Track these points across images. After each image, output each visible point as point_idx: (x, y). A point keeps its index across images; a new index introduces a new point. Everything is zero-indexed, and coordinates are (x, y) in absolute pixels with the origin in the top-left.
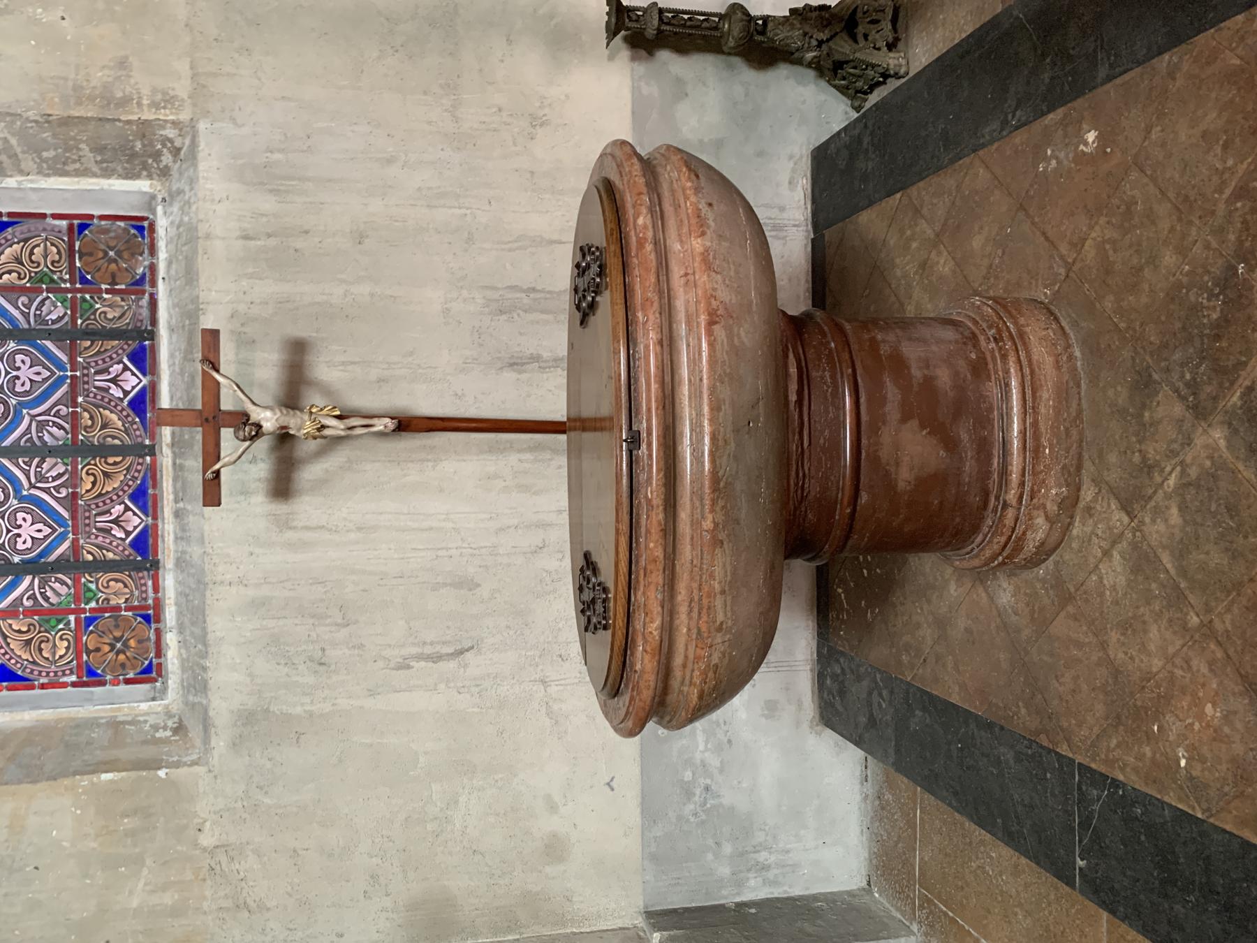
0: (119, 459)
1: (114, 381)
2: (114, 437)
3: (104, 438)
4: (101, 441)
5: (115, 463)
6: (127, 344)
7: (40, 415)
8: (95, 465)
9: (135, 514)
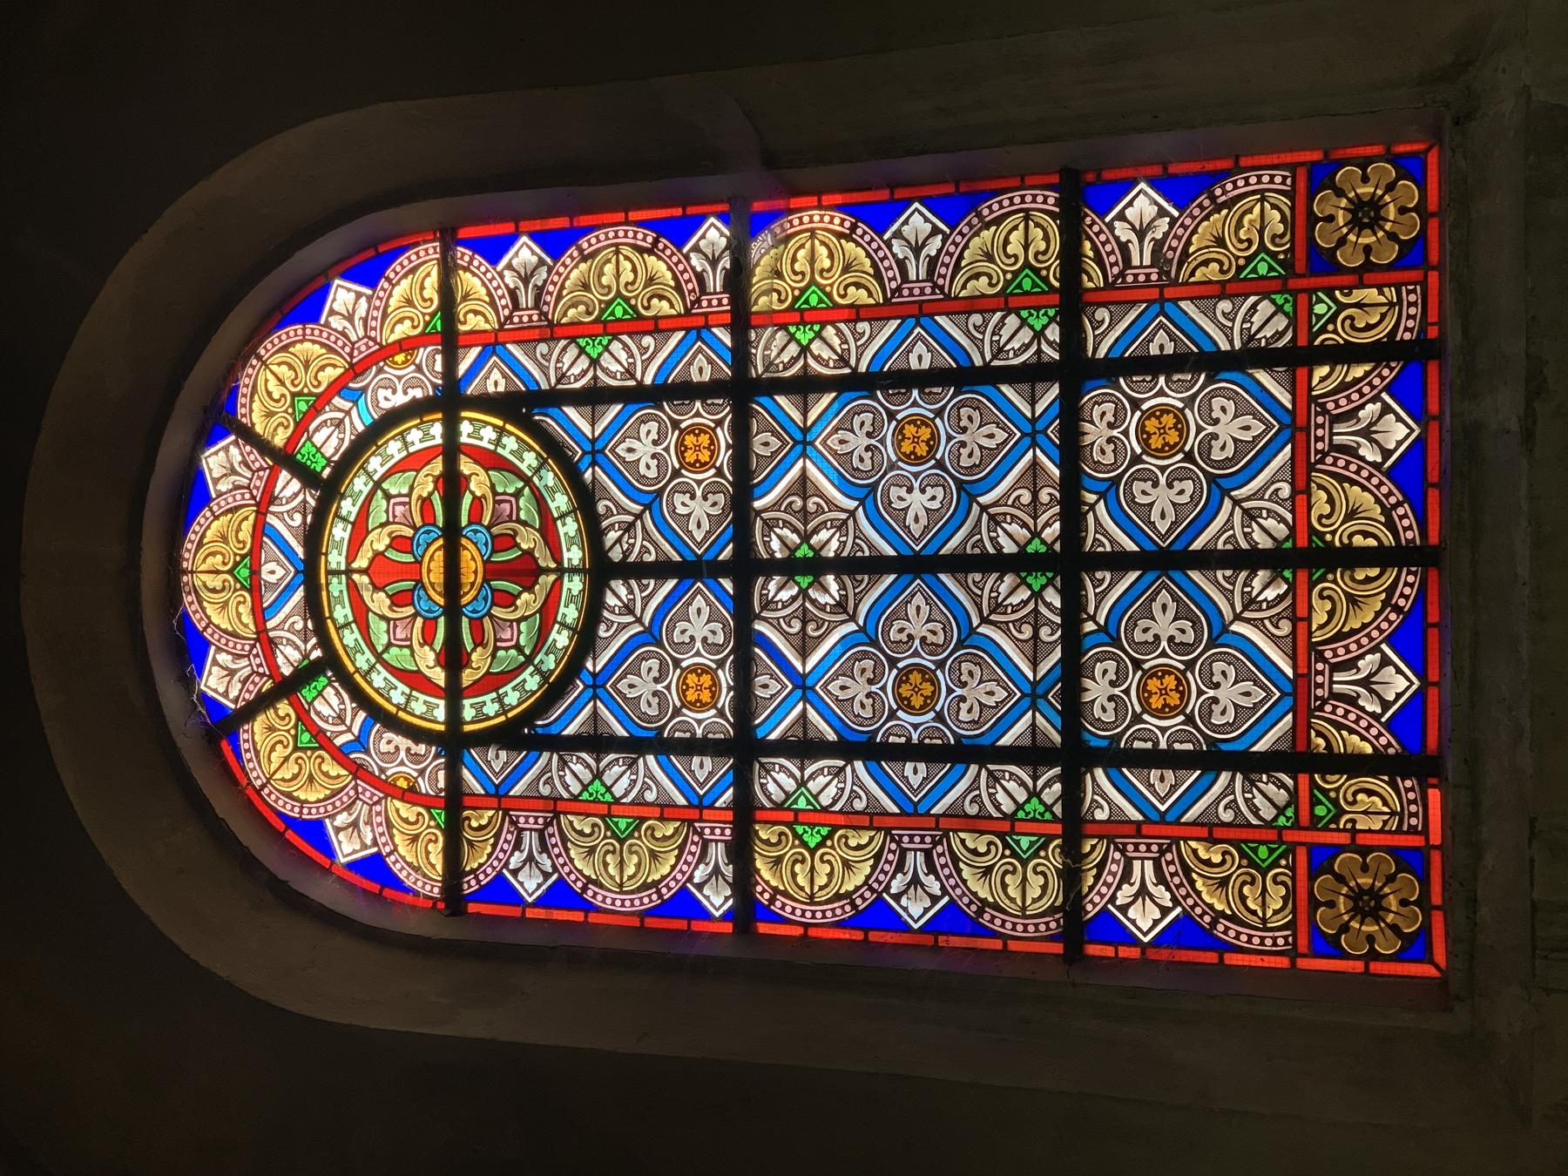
0: (1373, 572)
1: (1367, 433)
2: (1366, 534)
3: (1351, 536)
4: (1346, 541)
5: (1368, 580)
6: (1388, 366)
7: (1248, 499)
8: (1335, 581)
9: (1399, 671)
